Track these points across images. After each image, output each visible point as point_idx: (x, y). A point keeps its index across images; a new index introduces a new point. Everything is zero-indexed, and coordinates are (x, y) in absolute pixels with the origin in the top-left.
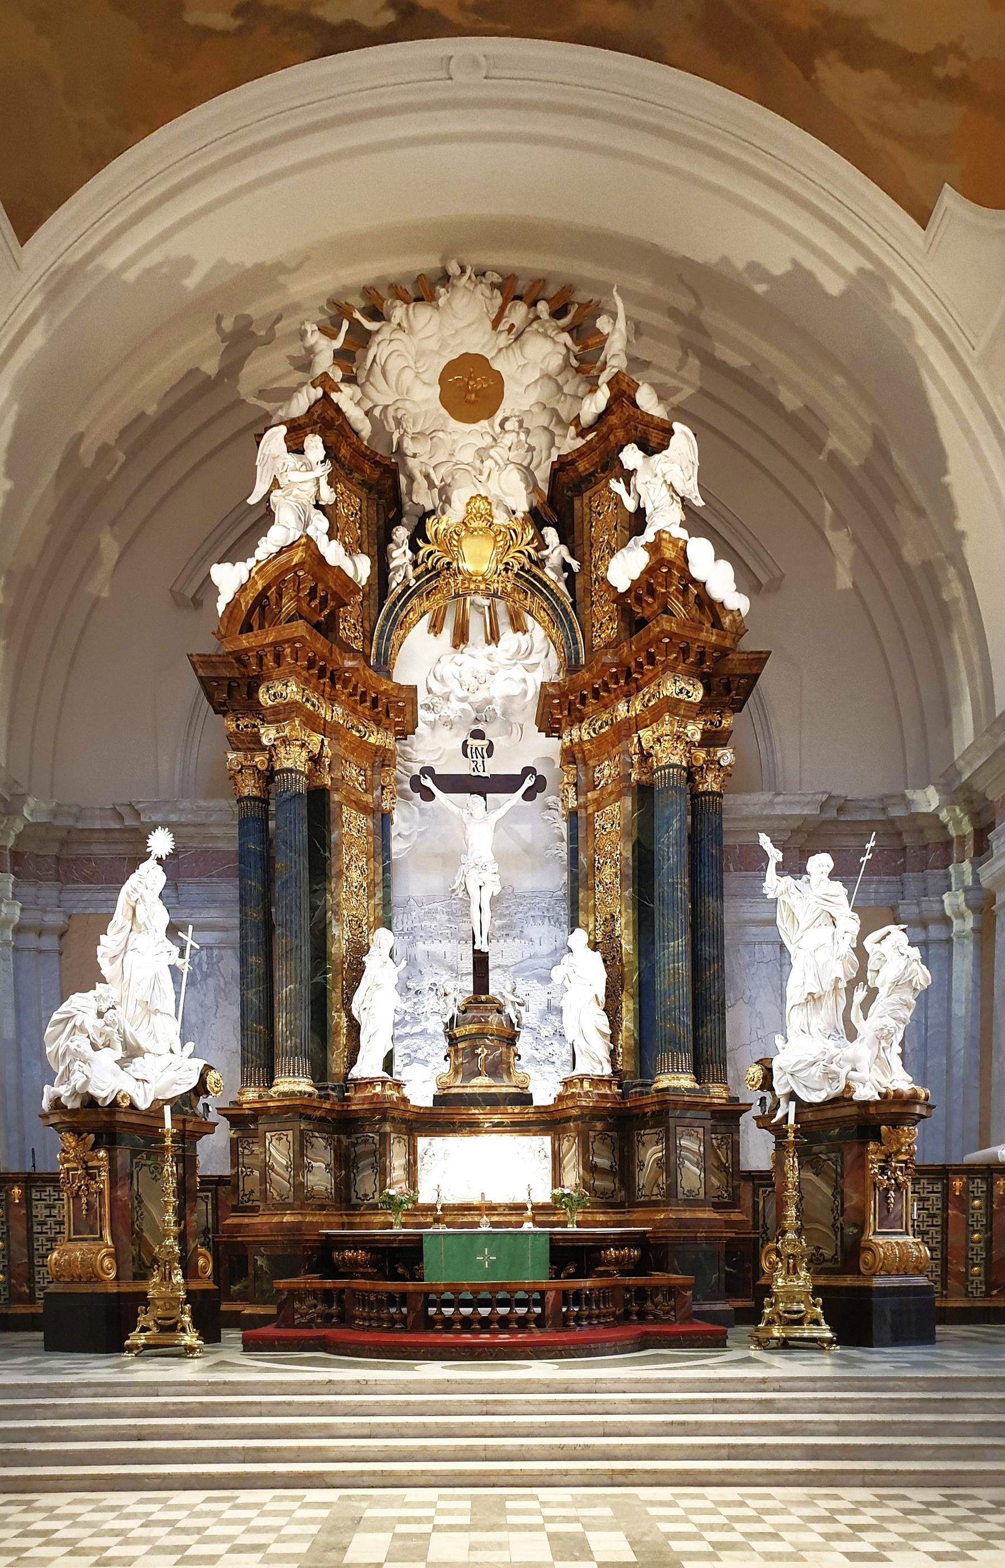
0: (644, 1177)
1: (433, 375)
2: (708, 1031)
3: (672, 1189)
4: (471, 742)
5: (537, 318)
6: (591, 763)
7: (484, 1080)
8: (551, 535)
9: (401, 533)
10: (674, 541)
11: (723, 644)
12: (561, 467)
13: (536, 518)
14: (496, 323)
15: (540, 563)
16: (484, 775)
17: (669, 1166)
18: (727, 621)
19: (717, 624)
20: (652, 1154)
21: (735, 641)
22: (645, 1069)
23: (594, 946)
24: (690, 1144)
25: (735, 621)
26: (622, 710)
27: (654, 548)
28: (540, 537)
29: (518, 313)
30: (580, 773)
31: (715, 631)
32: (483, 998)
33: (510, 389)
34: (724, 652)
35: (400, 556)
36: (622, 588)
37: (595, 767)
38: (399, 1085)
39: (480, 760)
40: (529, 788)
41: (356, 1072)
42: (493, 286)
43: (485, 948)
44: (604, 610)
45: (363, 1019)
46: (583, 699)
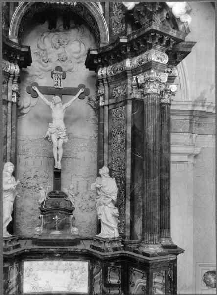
4: (55, 72)
6: (112, 86)
7: (57, 232)
11: (179, 38)
16: (61, 87)
18: (181, 27)
19: (176, 27)
21: (184, 37)
25: (185, 27)
26: (128, 64)
30: (106, 90)
31: (176, 31)
32: (58, 192)
34: (178, 41)
37: (113, 88)
39: (59, 81)
40: (82, 93)
43: (59, 167)
46: (109, 58)
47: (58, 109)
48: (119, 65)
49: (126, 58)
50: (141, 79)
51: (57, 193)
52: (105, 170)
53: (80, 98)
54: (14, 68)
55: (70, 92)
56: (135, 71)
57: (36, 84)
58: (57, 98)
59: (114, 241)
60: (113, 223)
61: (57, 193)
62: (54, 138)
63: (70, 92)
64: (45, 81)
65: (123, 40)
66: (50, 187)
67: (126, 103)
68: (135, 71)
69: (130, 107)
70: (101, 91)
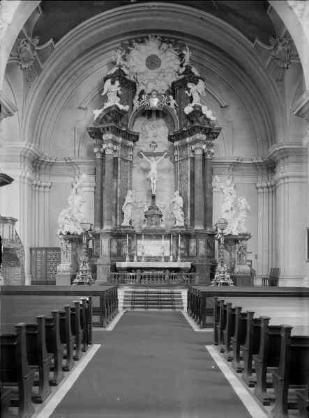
0: (192, 250)
1: (144, 59)
2: (208, 215)
3: (197, 253)
5: (169, 47)
8: (171, 97)
9: (137, 97)
10: (199, 106)
12: (173, 84)
13: (168, 93)
14: (159, 47)
15: (169, 104)
17: (197, 248)
20: (193, 244)
22: (192, 224)
23: (180, 195)
24: (202, 243)
27: (194, 107)
28: (169, 98)
29: (164, 46)
33: (162, 63)
35: (136, 102)
36: (187, 113)
38: (133, 228)
41: (123, 225)
42: (159, 40)
44: (182, 116)
45: (125, 212)
47: (154, 164)
48: (183, 141)
49: (187, 136)
50: (193, 147)
51: (153, 207)
52: (178, 192)
53: (165, 157)
54: (131, 143)
55: (160, 154)
56: (191, 144)
57: (142, 151)
58: (153, 158)
59: (182, 227)
60: (182, 219)
61: (153, 207)
62: (152, 179)
63: (160, 154)
64: (146, 148)
65: (185, 129)
66: (150, 204)
67: (187, 159)
68: (191, 144)
69: (189, 161)
70: (176, 153)
